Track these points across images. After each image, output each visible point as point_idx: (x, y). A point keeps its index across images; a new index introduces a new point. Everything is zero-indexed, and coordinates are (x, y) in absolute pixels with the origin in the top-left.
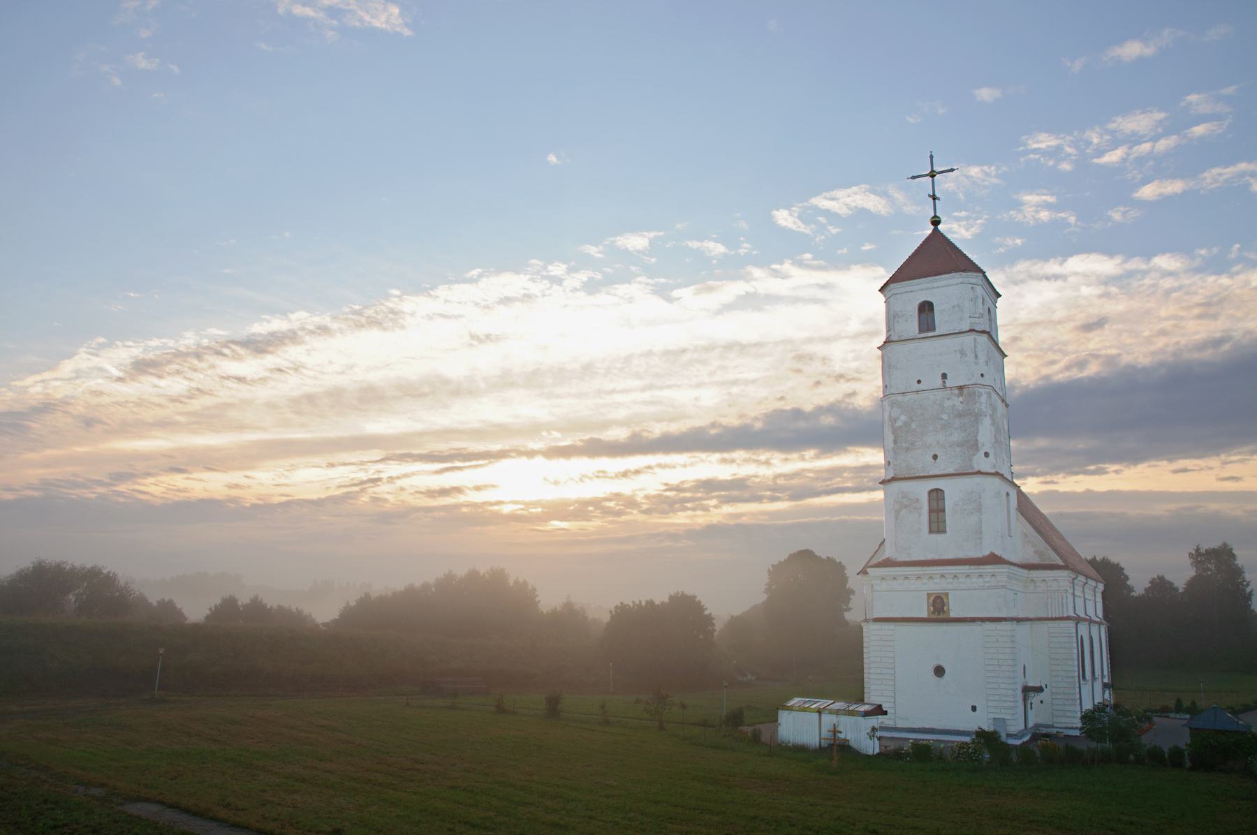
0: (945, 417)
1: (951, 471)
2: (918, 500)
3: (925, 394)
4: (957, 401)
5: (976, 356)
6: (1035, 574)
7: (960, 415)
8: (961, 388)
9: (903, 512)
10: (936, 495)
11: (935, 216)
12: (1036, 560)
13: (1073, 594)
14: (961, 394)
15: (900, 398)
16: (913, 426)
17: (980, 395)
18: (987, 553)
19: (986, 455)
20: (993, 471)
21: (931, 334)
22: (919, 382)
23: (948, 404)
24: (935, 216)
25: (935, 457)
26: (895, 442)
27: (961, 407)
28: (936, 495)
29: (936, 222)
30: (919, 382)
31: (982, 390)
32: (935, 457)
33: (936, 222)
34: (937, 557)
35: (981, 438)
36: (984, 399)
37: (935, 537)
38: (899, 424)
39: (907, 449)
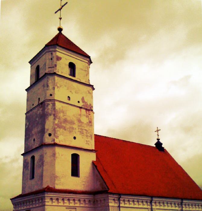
5: (48, 86)
6: (99, 197)
12: (100, 189)
13: (119, 207)
14: (42, 107)
16: (30, 127)
17: (49, 104)
18: (45, 186)
19: (50, 135)
20: (53, 143)
22: (33, 105)
29: (60, 30)
30: (33, 105)
31: (50, 103)
33: (60, 30)
35: (47, 127)
36: (50, 107)
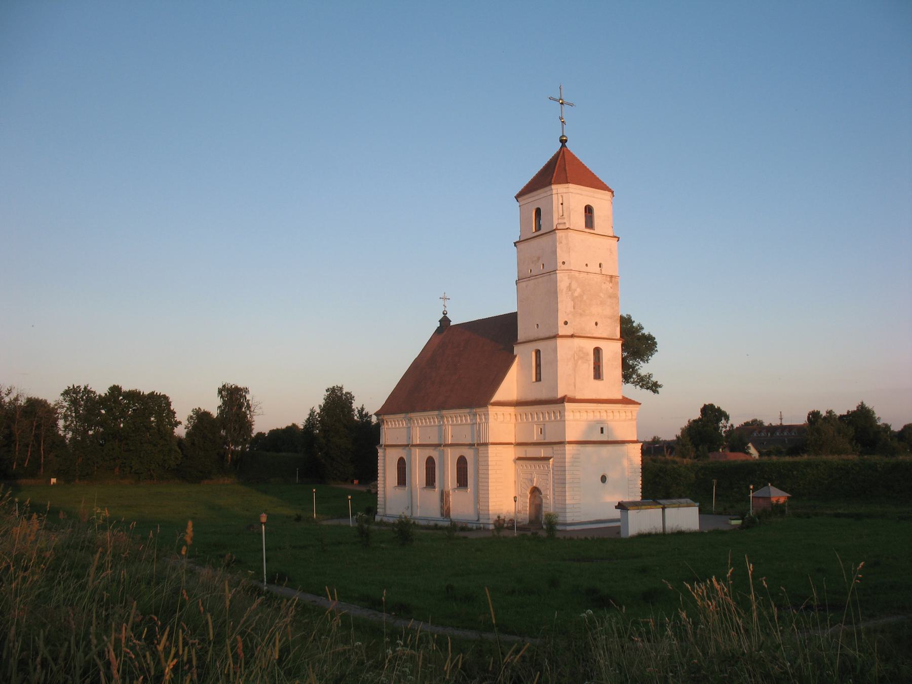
0: (602, 295)
1: (605, 336)
2: (588, 354)
3: (591, 276)
4: (608, 286)
7: (610, 297)
8: (611, 277)
9: (580, 362)
10: (597, 351)
11: (563, 136)
14: (611, 281)
15: (577, 274)
16: (585, 298)
21: (592, 231)
23: (604, 286)
24: (563, 136)
25: (596, 324)
26: (574, 308)
27: (611, 291)
28: (597, 351)
29: (563, 142)
32: (596, 324)
33: (563, 142)
34: (598, 397)
37: (597, 381)
38: (576, 294)
39: (581, 315)
